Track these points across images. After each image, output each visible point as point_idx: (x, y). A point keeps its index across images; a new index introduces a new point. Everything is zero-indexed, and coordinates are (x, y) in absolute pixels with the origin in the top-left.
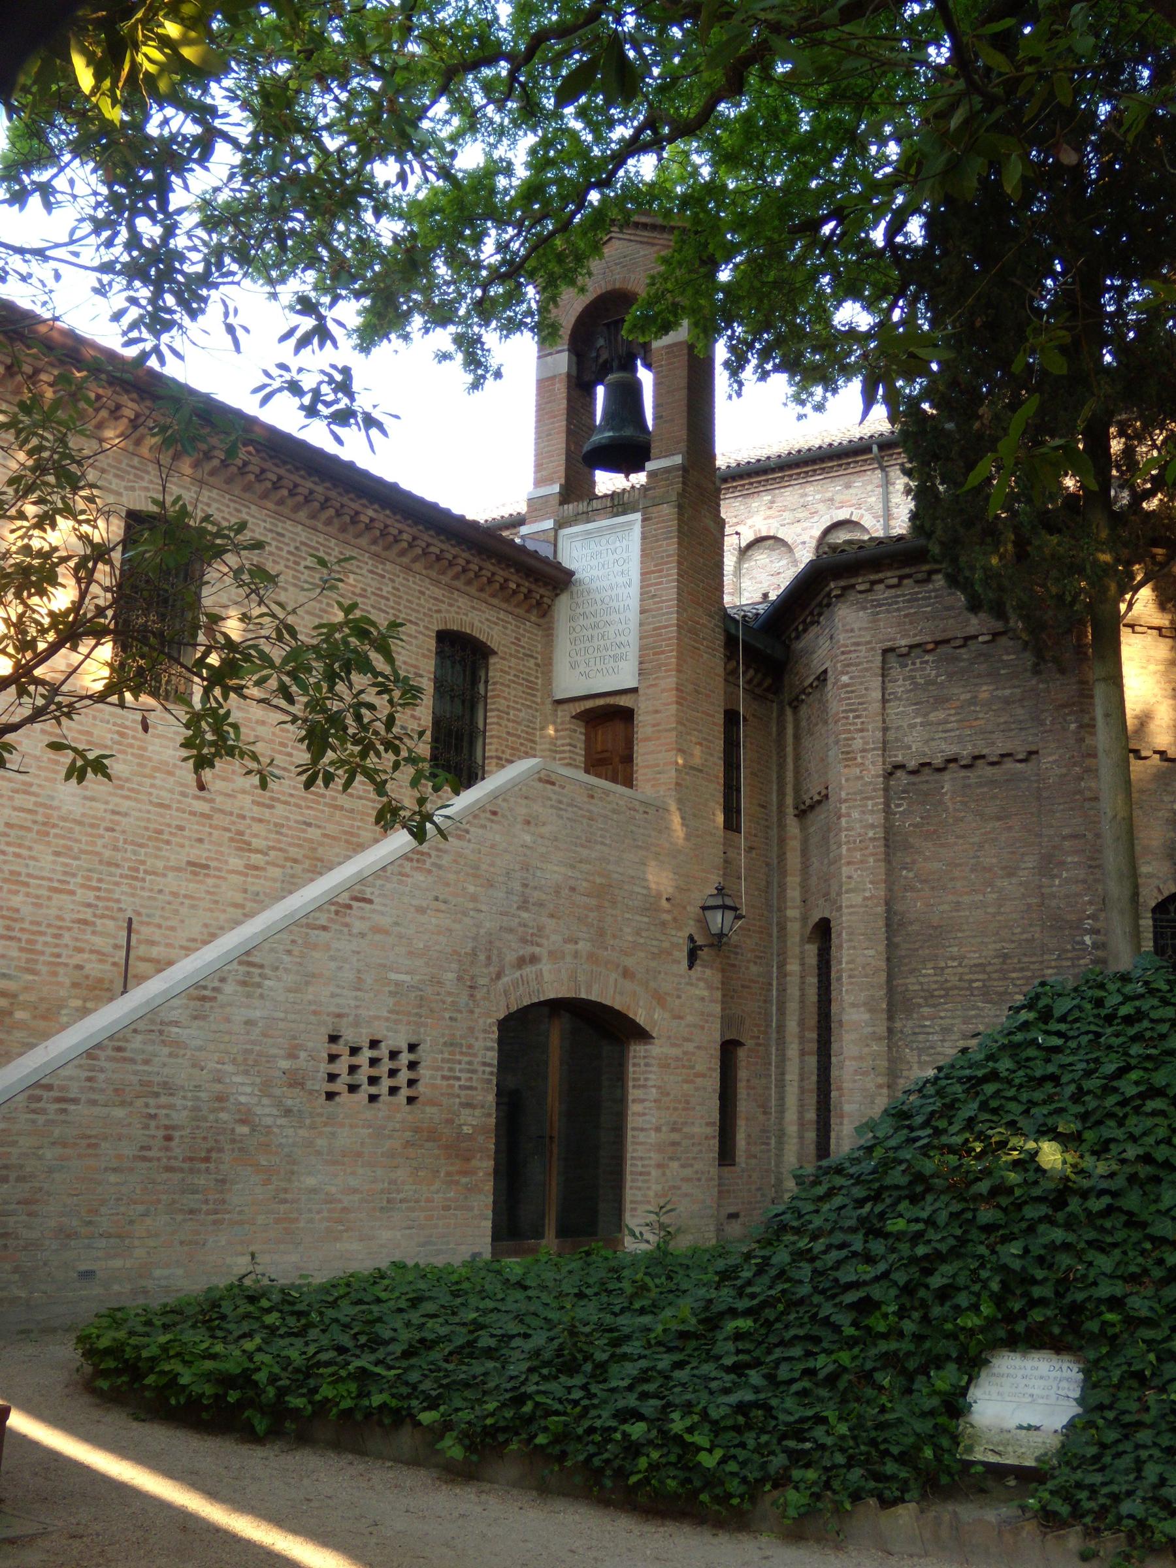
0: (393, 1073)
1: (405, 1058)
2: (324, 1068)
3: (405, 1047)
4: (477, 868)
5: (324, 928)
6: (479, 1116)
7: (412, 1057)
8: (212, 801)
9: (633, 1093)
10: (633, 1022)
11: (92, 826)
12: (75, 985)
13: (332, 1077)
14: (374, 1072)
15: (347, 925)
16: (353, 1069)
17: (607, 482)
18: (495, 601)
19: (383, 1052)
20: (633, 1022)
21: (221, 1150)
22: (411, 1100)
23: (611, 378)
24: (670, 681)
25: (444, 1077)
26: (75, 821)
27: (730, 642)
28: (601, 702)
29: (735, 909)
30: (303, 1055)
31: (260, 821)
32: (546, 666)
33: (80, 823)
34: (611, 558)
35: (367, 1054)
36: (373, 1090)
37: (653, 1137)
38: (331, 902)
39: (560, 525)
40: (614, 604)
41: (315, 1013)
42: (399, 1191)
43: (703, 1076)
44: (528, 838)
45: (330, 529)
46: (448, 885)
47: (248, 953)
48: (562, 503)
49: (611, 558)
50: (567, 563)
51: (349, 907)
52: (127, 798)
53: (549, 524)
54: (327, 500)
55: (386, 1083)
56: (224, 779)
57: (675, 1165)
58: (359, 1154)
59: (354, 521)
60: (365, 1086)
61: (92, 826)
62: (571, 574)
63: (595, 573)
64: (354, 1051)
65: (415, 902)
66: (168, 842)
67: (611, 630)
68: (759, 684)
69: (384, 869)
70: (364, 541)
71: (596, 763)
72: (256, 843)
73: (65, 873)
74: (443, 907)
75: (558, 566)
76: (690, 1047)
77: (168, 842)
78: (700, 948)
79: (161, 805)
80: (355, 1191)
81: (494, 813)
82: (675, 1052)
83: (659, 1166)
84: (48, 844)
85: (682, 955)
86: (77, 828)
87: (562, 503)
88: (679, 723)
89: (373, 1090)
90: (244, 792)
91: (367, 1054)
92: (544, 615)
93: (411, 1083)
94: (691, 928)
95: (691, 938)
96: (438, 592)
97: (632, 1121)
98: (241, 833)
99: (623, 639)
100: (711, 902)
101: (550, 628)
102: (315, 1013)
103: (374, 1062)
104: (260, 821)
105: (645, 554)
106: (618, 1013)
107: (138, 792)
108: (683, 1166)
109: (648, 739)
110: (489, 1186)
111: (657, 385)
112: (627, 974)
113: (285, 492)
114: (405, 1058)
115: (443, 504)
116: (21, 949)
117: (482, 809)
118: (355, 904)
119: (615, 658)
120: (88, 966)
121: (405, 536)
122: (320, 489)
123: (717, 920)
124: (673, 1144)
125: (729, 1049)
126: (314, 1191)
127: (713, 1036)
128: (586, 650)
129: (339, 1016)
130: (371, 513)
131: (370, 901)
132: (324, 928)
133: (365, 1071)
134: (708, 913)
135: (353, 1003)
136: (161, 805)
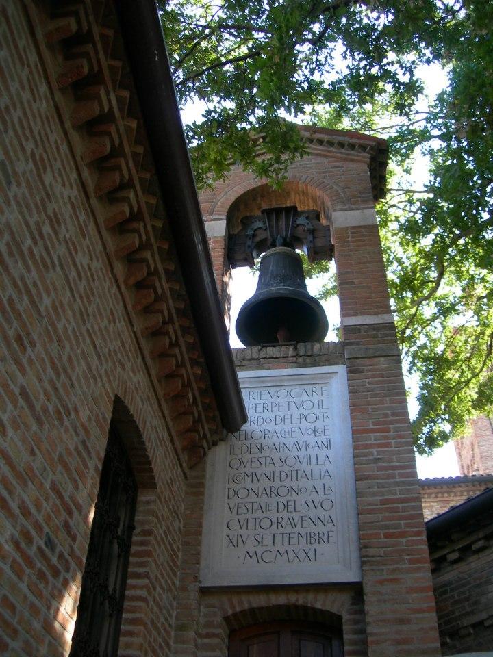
28: (281, 599)
34: (296, 413)
40: (304, 467)
49: (296, 413)
63: (270, 427)
67: (301, 499)
99: (320, 512)
101: (202, 485)
119: (309, 538)
128: (258, 524)
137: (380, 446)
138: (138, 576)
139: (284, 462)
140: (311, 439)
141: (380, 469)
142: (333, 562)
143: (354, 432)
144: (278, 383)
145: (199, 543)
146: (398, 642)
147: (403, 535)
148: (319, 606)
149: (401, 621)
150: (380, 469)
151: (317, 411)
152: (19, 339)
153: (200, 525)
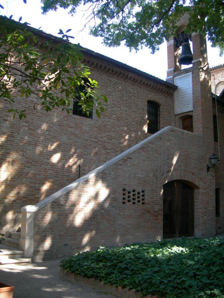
0: (138, 197)
1: (141, 194)
2: (122, 196)
3: (141, 191)
4: (157, 151)
5: (121, 165)
6: (159, 207)
7: (143, 194)
8: (98, 139)
9: (196, 201)
10: (195, 185)
11: (70, 145)
12: (67, 180)
13: (124, 199)
14: (134, 197)
15: (126, 164)
16: (129, 197)
17: (184, 67)
18: (160, 94)
19: (136, 193)
20: (195, 184)
21: (98, 216)
22: (143, 203)
23: (183, 44)
24: (200, 108)
25: (151, 198)
26: (67, 144)
27: (214, 99)
28: (185, 114)
29: (217, 158)
30: (117, 193)
31: (109, 143)
32: (173, 107)
33: (67, 144)
34: (186, 83)
35: (132, 193)
36: (134, 201)
37: (200, 210)
38: (122, 159)
39: (174, 77)
41: (119, 184)
42: (140, 224)
43: (212, 196)
44: (168, 144)
45: (122, 79)
46: (150, 155)
47: (103, 171)
48: (174, 72)
49: (186, 83)
50: (176, 84)
51: (127, 160)
52: (78, 138)
53: (172, 77)
54: (120, 73)
55: (137, 200)
56: (100, 134)
57: (205, 217)
58: (131, 216)
59: (127, 76)
60: (132, 200)
61: (70, 145)
62: (177, 87)
63: (182, 86)
64: (129, 193)
65: (142, 159)
66: (88, 148)
68: (221, 109)
69: (135, 151)
70: (129, 81)
71: (185, 128)
72: (108, 148)
73: (64, 155)
74: (149, 160)
75: (174, 86)
76: (208, 190)
77: (88, 148)
78: (210, 168)
79: (86, 140)
80: (130, 224)
81: (160, 138)
82: (205, 191)
83: (202, 217)
84: (60, 149)
85: (206, 169)
86: (67, 145)
87: (174, 72)
88: (203, 117)
89: (134, 201)
90: (105, 136)
91: (132, 193)
92: (172, 96)
93: (143, 199)
94: (208, 163)
95: (208, 166)
96: (147, 92)
97: (195, 207)
98: (105, 146)
100: (212, 157)
102: (119, 184)
103: (134, 195)
104: (109, 143)
105: (193, 81)
106: (191, 182)
107: (81, 137)
108: (207, 217)
109: (196, 122)
110: (162, 223)
111: (193, 44)
112: (193, 174)
113: (111, 71)
114: (141, 194)
115: (147, 72)
116: (55, 172)
117: (157, 137)
118: (128, 159)
119: (188, 104)
120: (70, 176)
121: (139, 80)
122: (119, 70)
123: (213, 161)
124: (205, 212)
125: (217, 191)
126: (120, 224)
127: (214, 187)
129: (125, 185)
130: (131, 75)
131: (132, 159)
132: (121, 165)
133: (132, 197)
134: (211, 160)
135: (128, 182)
136: (86, 140)
137: (196, 87)
138: (161, 117)
139: (184, 92)
140: (188, 87)
141: (196, 91)
142: (190, 108)
143: (193, 85)
144: (183, 77)
145: (174, 108)
146: (197, 118)
147: (198, 102)
148: (190, 114)
149: (197, 115)
150: (196, 91)
151: (188, 82)
152: (130, 107)
153: (174, 106)
